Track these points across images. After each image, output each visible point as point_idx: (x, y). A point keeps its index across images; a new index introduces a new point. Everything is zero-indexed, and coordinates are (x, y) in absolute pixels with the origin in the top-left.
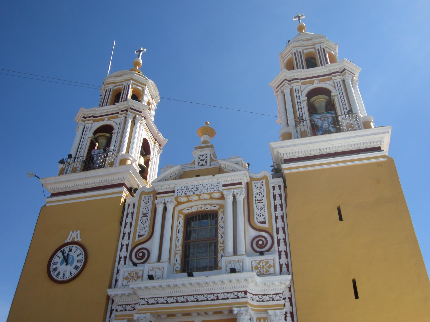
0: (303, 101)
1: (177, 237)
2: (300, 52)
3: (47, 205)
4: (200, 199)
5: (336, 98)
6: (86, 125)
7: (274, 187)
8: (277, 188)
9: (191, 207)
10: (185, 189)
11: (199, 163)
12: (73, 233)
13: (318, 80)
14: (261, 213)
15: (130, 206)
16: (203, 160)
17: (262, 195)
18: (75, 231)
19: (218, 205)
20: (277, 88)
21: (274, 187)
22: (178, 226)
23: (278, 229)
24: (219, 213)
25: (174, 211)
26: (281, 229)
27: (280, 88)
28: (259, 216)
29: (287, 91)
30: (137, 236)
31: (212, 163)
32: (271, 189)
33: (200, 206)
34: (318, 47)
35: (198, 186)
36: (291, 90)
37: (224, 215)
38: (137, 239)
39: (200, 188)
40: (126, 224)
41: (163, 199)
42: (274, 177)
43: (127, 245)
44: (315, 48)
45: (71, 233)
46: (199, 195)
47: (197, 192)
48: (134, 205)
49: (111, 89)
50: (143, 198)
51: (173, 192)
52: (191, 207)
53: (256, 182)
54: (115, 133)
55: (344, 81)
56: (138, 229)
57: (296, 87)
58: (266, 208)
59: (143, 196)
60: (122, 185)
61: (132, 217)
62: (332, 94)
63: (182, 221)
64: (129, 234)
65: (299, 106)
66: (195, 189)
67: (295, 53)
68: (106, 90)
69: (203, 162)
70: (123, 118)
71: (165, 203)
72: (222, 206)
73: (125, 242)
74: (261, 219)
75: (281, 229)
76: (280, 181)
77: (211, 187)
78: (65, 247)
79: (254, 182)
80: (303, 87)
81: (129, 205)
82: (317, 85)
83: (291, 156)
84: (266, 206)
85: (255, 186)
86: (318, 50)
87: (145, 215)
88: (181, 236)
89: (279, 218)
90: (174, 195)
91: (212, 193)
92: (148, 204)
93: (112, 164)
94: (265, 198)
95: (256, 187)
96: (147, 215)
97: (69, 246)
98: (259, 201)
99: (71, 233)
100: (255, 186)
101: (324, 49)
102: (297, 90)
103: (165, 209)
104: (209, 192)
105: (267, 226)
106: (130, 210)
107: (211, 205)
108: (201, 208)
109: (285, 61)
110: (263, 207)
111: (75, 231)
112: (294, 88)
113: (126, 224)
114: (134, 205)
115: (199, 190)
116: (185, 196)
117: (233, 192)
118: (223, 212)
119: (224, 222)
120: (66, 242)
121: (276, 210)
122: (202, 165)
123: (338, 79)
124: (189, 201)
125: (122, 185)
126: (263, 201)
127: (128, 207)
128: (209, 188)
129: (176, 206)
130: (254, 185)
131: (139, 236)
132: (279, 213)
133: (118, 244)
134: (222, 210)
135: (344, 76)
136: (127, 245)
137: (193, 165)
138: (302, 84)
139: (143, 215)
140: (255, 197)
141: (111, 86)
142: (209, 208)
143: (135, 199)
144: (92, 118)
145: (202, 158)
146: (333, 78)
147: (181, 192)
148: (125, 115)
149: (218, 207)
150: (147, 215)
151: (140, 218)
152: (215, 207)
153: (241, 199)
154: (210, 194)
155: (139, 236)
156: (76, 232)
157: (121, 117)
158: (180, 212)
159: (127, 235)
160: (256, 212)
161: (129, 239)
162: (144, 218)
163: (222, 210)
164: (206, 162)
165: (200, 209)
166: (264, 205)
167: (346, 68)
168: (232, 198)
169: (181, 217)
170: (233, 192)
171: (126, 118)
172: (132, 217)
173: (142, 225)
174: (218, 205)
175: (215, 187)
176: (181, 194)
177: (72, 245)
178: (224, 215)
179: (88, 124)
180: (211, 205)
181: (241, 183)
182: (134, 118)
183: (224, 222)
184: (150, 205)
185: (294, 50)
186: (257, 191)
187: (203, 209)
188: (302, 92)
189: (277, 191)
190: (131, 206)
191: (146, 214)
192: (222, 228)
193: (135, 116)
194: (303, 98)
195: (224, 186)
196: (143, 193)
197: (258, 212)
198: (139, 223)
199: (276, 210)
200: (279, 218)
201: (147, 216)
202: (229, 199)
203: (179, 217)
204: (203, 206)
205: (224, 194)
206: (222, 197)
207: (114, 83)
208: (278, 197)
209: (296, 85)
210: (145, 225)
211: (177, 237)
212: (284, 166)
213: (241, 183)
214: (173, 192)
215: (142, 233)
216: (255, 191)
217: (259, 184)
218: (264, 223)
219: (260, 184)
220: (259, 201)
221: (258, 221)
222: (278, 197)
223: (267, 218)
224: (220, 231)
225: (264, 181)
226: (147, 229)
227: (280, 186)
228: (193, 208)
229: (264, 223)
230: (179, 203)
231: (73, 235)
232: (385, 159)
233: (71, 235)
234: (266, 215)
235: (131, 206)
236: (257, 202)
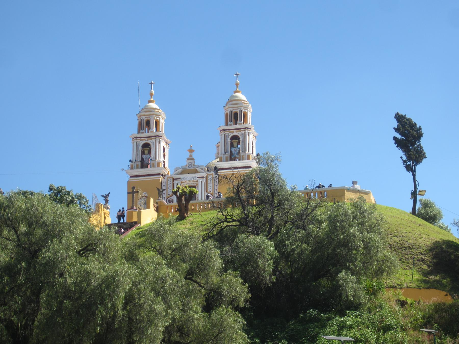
14: (210, 188)
29: (223, 136)
34: (239, 109)
51: (180, 179)
60: (159, 174)
72: (197, 184)
73: (164, 196)
82: (235, 134)
87: (170, 187)
105: (212, 192)
106: (164, 184)
125: (159, 174)
132: (216, 188)
140: (209, 182)
141: (144, 117)
143: (165, 180)
153: (203, 183)
160: (209, 187)
184: (171, 182)
195: (198, 177)
196: (168, 177)
206: (197, 181)
207: (145, 115)
214: (180, 179)
216: (208, 179)
230: (182, 183)
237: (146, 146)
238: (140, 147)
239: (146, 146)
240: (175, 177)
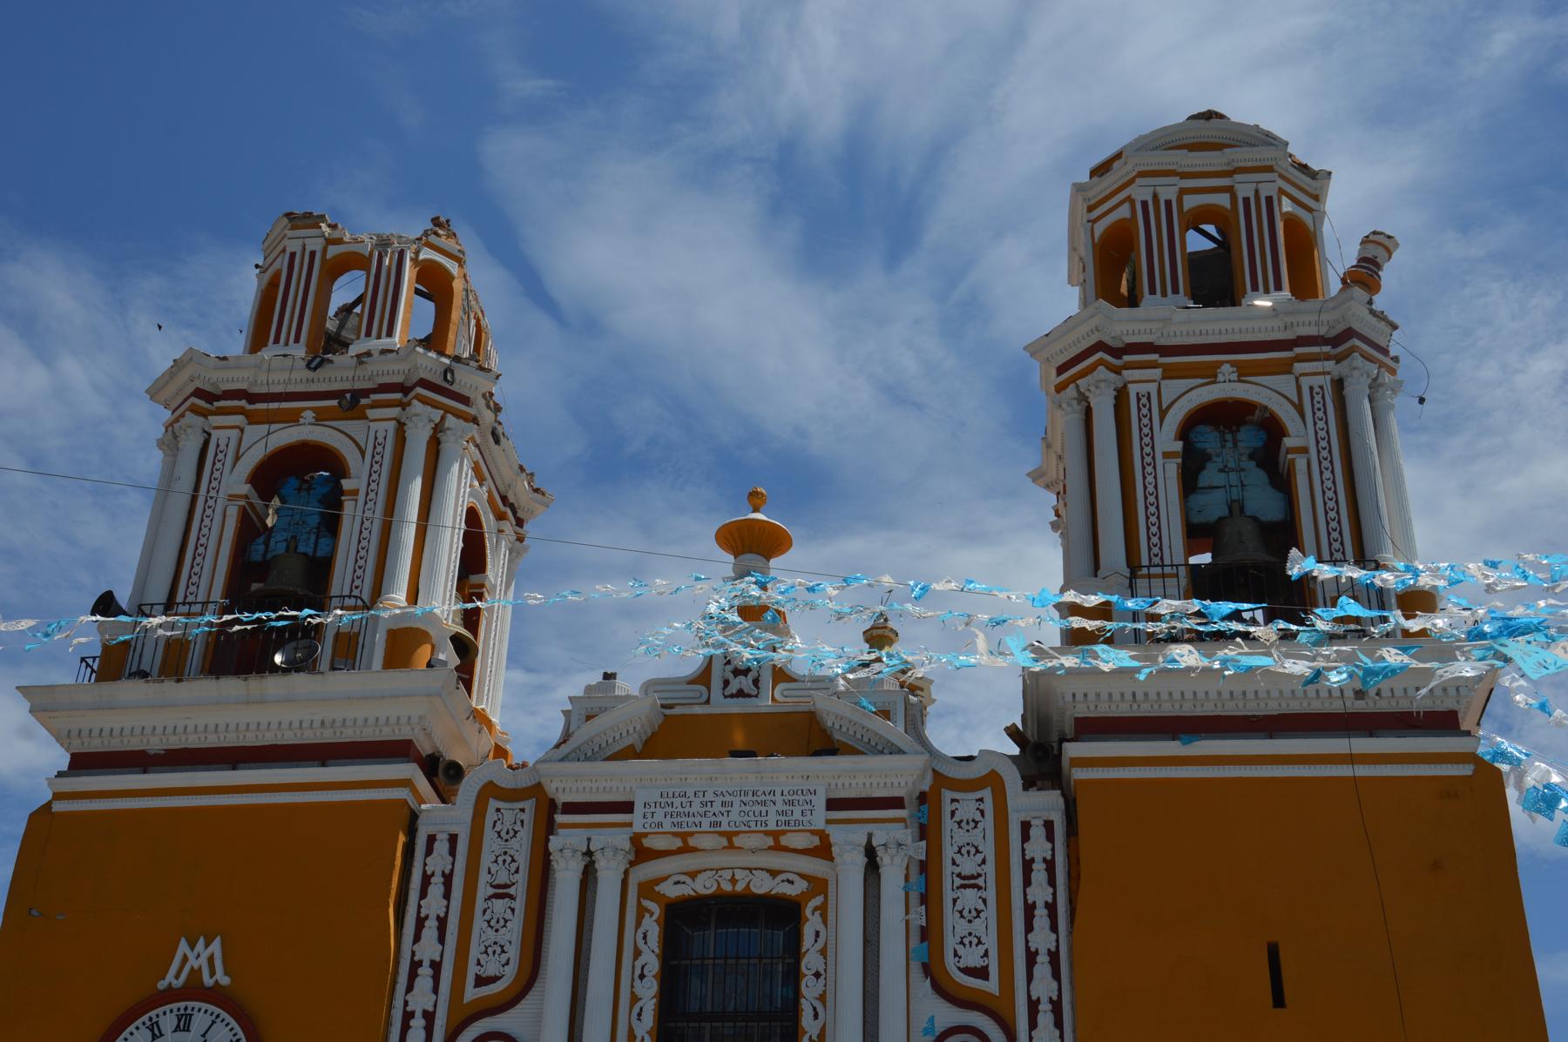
0: (1167, 455)
1: (635, 999)
2: (1168, 203)
3: (58, 807)
4: (731, 846)
5: (1300, 464)
6: (215, 434)
7: (1026, 827)
8: (1037, 832)
9: (693, 875)
10: (677, 802)
11: (726, 683)
12: (192, 947)
13: (1233, 363)
15: (437, 845)
17: (979, 857)
18: (201, 941)
19: (802, 876)
20: (1061, 370)
21: (1026, 827)
22: (637, 953)
23: (1033, 1006)
24: (808, 912)
25: (625, 883)
26: (1045, 1007)
27: (1073, 379)
28: (961, 942)
30: (470, 980)
31: (780, 687)
33: (727, 874)
34: (1244, 190)
35: (728, 798)
36: (1121, 397)
37: (825, 922)
38: (471, 993)
39: (736, 801)
40: (420, 922)
41: (584, 833)
42: (1029, 783)
43: (429, 1017)
44: (1230, 190)
45: (183, 947)
46: (729, 836)
47: (724, 820)
48: (453, 839)
49: (313, 254)
51: (627, 807)
52: (693, 875)
53: (957, 795)
54: (356, 492)
55: (1339, 384)
56: (475, 952)
57: (1143, 388)
58: (991, 912)
59: (493, 804)
61: (447, 895)
62: (1288, 442)
63: (652, 928)
64: (436, 966)
65: (1150, 479)
66: (717, 807)
67: (1145, 204)
68: (293, 255)
69: (745, 683)
70: (391, 425)
71: (589, 853)
72: (818, 886)
73: (421, 999)
74: (972, 958)
75: (1045, 1007)
76: (1048, 803)
77: (780, 807)
78: (160, 1010)
79: (947, 795)
80: (1173, 387)
82: (1227, 388)
83: (1104, 710)
84: (992, 902)
85: (953, 813)
86: (1246, 201)
87: (501, 892)
89: (1043, 959)
90: (630, 825)
91: (784, 832)
92: (514, 843)
93: (348, 650)
94: (990, 868)
95: (957, 818)
96: (512, 891)
97: (174, 1006)
98: (970, 882)
99: (183, 947)
100: (953, 813)
101: (1269, 200)
102: (1144, 401)
103: (589, 877)
104: (772, 826)
105: (992, 986)
106: (439, 861)
107: (774, 873)
108: (733, 881)
109: (1100, 228)
110: (981, 906)
111: (201, 941)
112: (1133, 389)
113: (420, 922)
114: (453, 839)
115: (734, 816)
116: (675, 834)
117: (870, 836)
118: (823, 910)
119: (823, 952)
120: (162, 985)
122: (741, 693)
123: (1315, 374)
124: (686, 849)
126: (980, 881)
128: (772, 809)
129: (632, 864)
130: (947, 808)
131: (481, 981)
133: (390, 1007)
134: (818, 901)
135: (1345, 363)
136: (429, 1017)
137: (703, 688)
138: (1170, 373)
139: (491, 891)
142: (762, 885)
144: (243, 403)
146: (1299, 367)
147: (659, 817)
148: (394, 412)
149: (800, 886)
150: (512, 891)
151: (480, 904)
152: (792, 882)
154: (776, 835)
155: (481, 981)
156: (207, 946)
157: (380, 423)
158: (648, 889)
159: (425, 971)
161: (436, 990)
162: (499, 905)
163: (818, 901)
164: (756, 682)
165: (727, 887)
166: (985, 901)
167: (1356, 326)
168: (861, 860)
169: (652, 914)
170: (870, 836)
171: (401, 427)
172: (447, 895)
173: (490, 932)
174: (802, 876)
175: (797, 810)
176: (660, 825)
177: (190, 1004)
178: (825, 922)
179: (225, 430)
180: (774, 873)
181: (897, 803)
182: (438, 429)
183: (823, 952)
185: (1141, 192)
186: (961, 837)
187: (739, 887)
188: (1163, 414)
189: (1038, 847)
190: (441, 847)
191: (506, 886)
192: (817, 975)
193: (443, 418)
194: (1167, 439)
195: (832, 804)
196: (490, 791)
197: (962, 927)
198: (479, 923)
199: (1029, 928)
200: (1043, 959)
201: (512, 897)
202: (851, 866)
203: (641, 912)
204: (739, 874)
205: (832, 840)
206: (823, 850)
208: (1039, 874)
209: (1142, 381)
211: (635, 999)
212: (1073, 750)
213: (897, 803)
214: (627, 807)
215: (491, 970)
216: (952, 837)
217: (967, 809)
218: (982, 973)
219: (974, 805)
220: (970, 882)
221: (962, 965)
222: (1039, 874)
223: (993, 954)
224: (810, 989)
225: (986, 793)
226: (513, 952)
227: (1049, 825)
228: (701, 878)
229: (982, 973)
231: (191, 956)
232: (1466, 770)
233: (185, 959)
234: (991, 942)
235: (441, 847)
236: (958, 882)
237: (304, 474)
238: (236, 481)
239: (304, 474)
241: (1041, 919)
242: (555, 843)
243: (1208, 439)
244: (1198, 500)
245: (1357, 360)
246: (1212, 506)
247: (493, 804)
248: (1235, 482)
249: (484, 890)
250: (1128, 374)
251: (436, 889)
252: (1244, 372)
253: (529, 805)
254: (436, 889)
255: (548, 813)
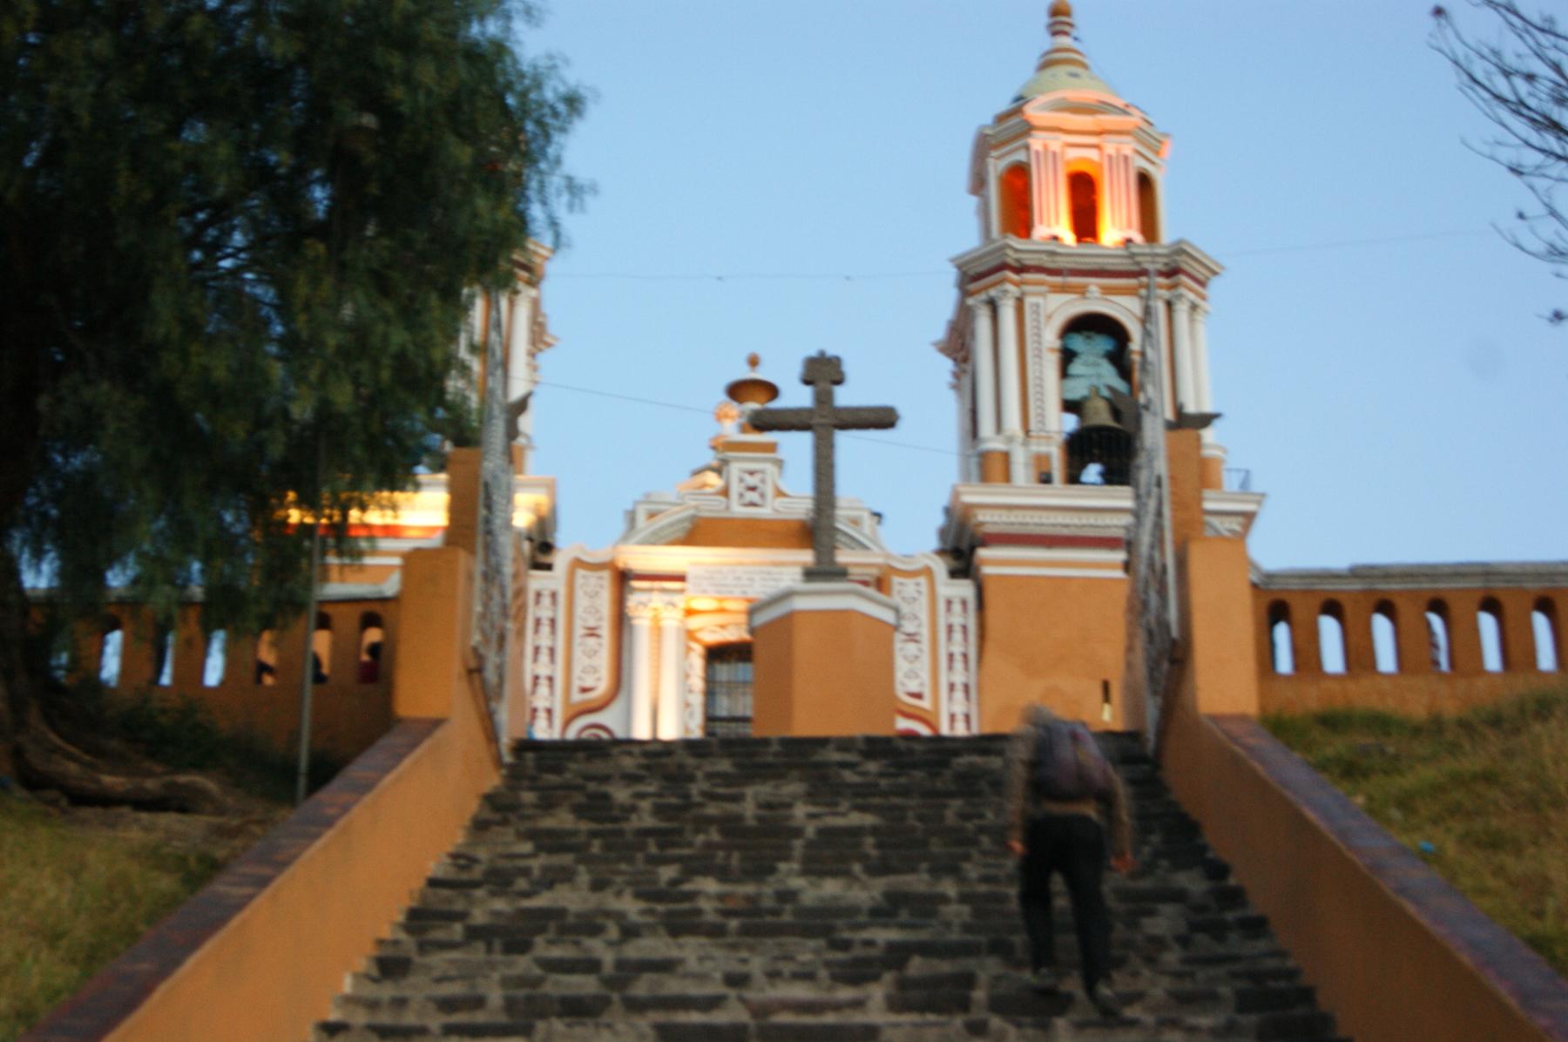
1: (687, 705)
7: (949, 603)
8: (957, 607)
16: (753, 489)
32: (942, 606)
38: (577, 697)
42: (954, 574)
50: (579, 581)
58: (926, 659)
63: (697, 662)
74: (913, 686)
76: (965, 589)
81: (538, 595)
82: (1096, 303)
87: (592, 633)
88: (697, 700)
105: (926, 704)
112: (1029, 300)
114: (554, 595)
121: (950, 668)
127: (537, 602)
131: (584, 690)
145: (752, 481)
151: (577, 640)
159: (543, 683)
162: (592, 641)
188: (1049, 317)
190: (546, 601)
194: (1051, 337)
208: (958, 636)
210: (596, 661)
215: (588, 683)
218: (918, 696)
227: (964, 603)
229: (918, 696)
234: (925, 676)
235: (546, 601)
240: (641, 558)
241: (959, 665)
242: (633, 601)
243: (1077, 343)
244: (1070, 383)
245: (1183, 291)
246: (1077, 390)
247: (581, 572)
248: (1095, 373)
249: (579, 631)
250: (1026, 288)
251: (545, 629)
252: (1108, 291)
253: (606, 575)
254: (545, 629)
255: (623, 579)
